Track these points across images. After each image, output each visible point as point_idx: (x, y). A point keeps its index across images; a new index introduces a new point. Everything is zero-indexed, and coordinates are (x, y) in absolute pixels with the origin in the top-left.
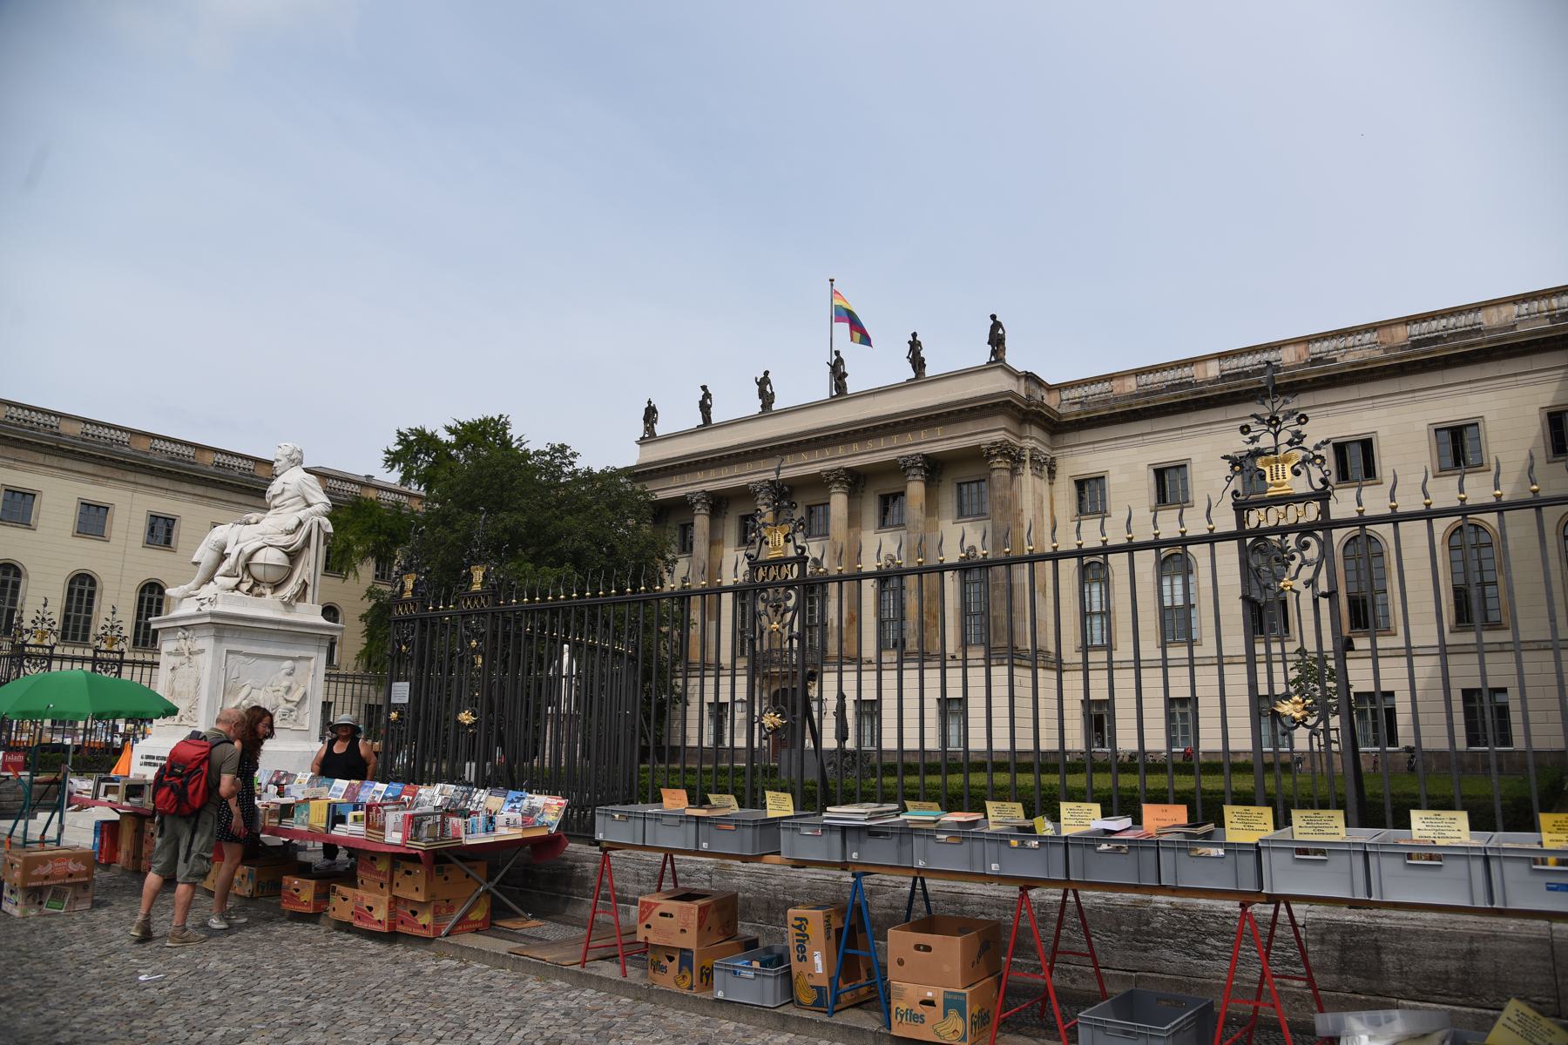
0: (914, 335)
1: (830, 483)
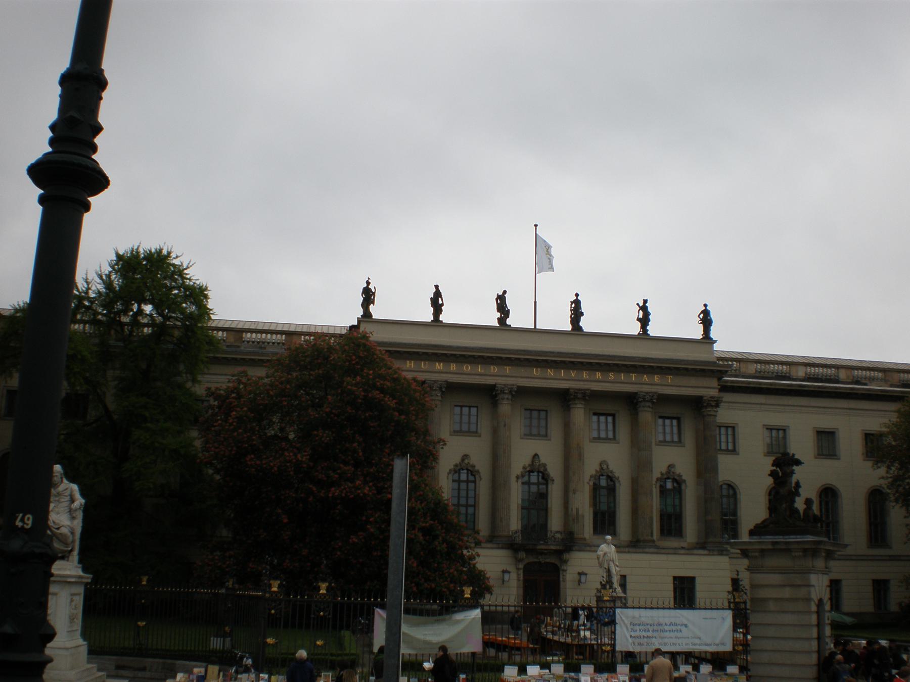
0: (645, 301)
1: (576, 398)
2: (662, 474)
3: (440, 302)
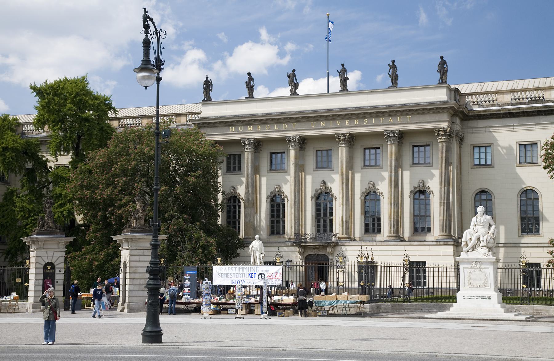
2: (415, 188)
3: (252, 84)
